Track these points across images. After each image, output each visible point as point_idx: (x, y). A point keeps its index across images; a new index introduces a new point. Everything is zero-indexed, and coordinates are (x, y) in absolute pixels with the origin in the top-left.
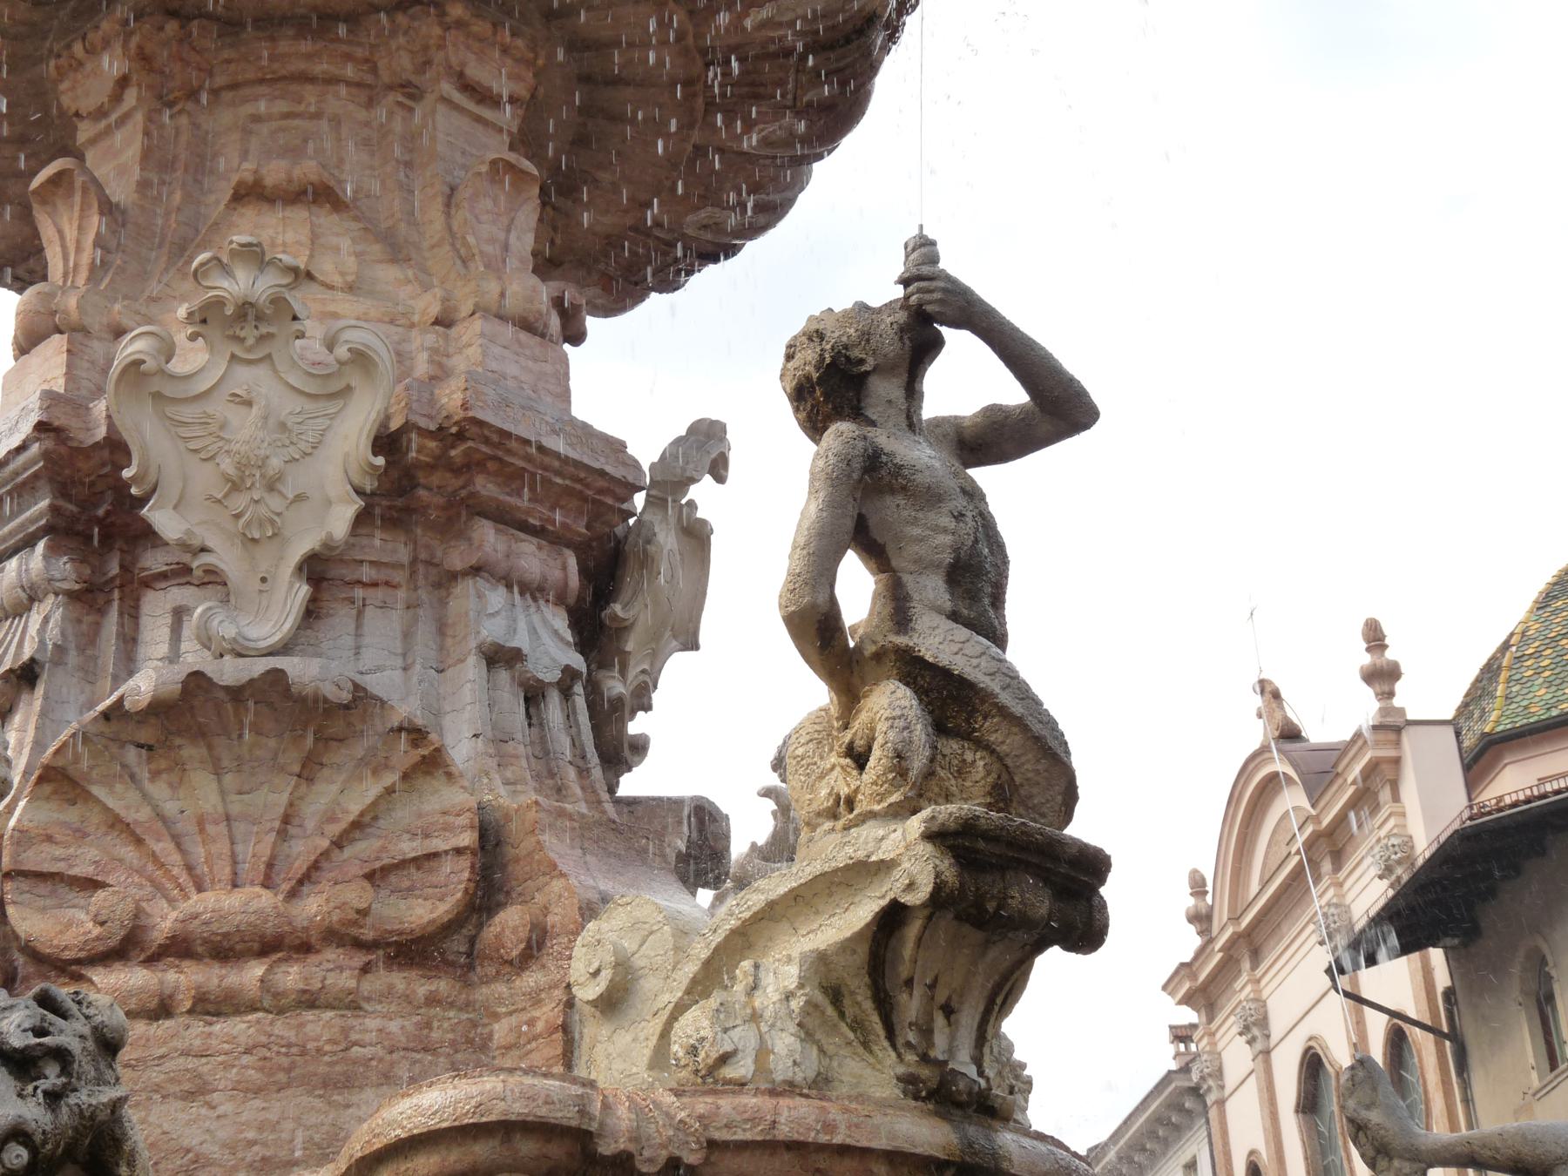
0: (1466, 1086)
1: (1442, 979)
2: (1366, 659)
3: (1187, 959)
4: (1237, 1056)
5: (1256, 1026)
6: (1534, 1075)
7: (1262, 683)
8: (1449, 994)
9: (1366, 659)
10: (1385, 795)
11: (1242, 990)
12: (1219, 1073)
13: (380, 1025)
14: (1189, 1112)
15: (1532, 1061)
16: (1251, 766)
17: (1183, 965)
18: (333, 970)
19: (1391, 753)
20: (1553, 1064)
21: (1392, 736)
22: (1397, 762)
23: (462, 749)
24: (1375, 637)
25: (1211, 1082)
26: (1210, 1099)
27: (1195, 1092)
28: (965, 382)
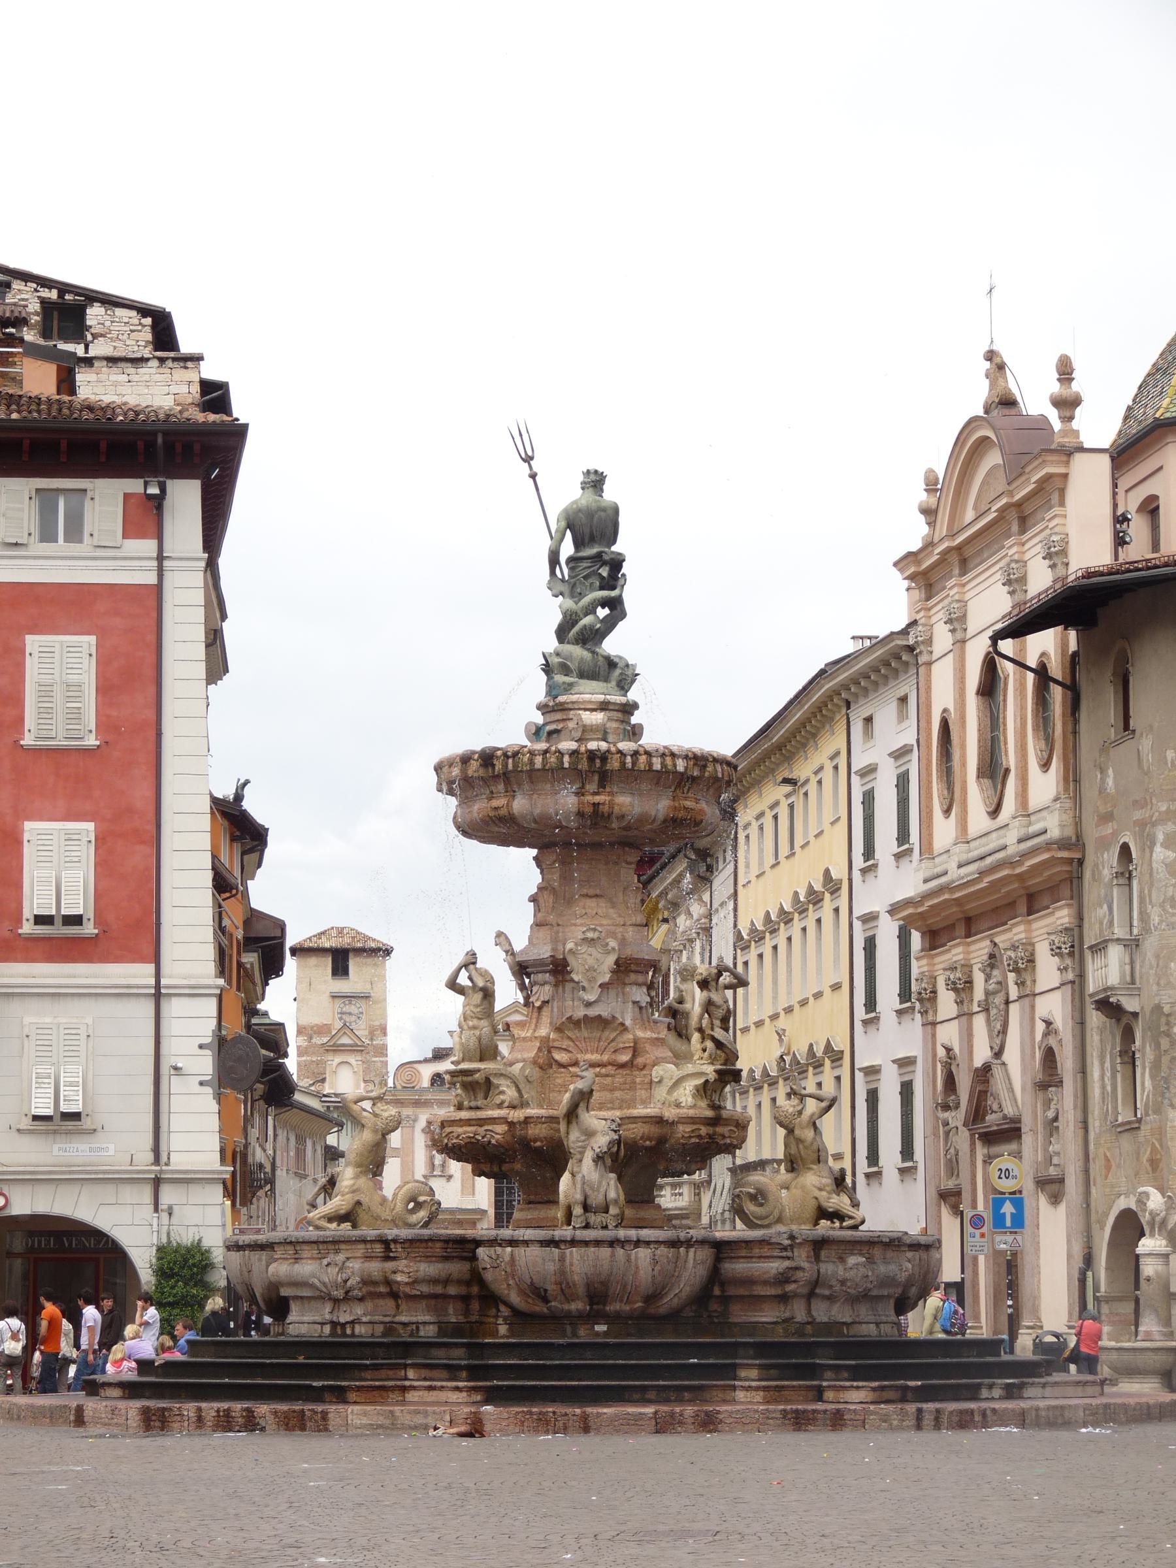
0: (1076, 722)
1: (1073, 646)
2: (1055, 388)
3: (914, 550)
4: (943, 639)
5: (957, 621)
6: (1113, 730)
7: (990, 355)
8: (1075, 655)
9: (1055, 388)
10: (1055, 497)
11: (951, 589)
12: (929, 642)
13: (619, 1080)
14: (907, 663)
15: (1113, 721)
16: (973, 425)
17: (910, 554)
18: (610, 1069)
19: (1062, 470)
20: (1126, 727)
21: (1064, 458)
22: (1065, 476)
23: (628, 1023)
24: (1065, 371)
25: (922, 647)
26: (922, 659)
27: (911, 649)
28: (726, 978)
